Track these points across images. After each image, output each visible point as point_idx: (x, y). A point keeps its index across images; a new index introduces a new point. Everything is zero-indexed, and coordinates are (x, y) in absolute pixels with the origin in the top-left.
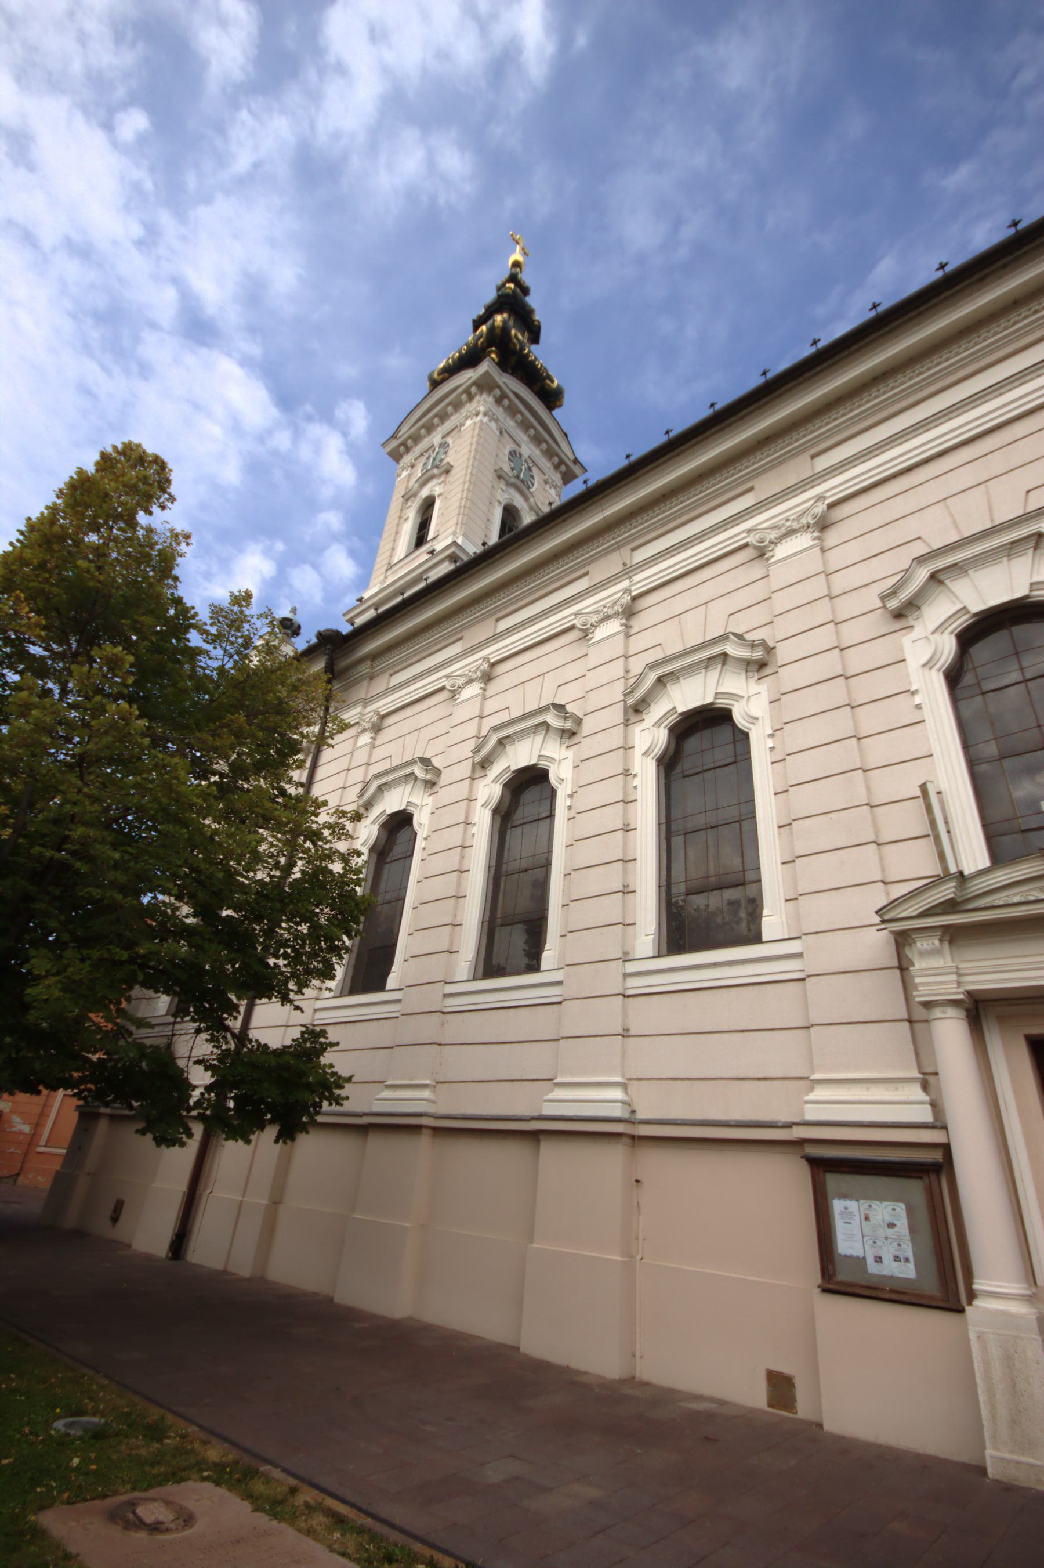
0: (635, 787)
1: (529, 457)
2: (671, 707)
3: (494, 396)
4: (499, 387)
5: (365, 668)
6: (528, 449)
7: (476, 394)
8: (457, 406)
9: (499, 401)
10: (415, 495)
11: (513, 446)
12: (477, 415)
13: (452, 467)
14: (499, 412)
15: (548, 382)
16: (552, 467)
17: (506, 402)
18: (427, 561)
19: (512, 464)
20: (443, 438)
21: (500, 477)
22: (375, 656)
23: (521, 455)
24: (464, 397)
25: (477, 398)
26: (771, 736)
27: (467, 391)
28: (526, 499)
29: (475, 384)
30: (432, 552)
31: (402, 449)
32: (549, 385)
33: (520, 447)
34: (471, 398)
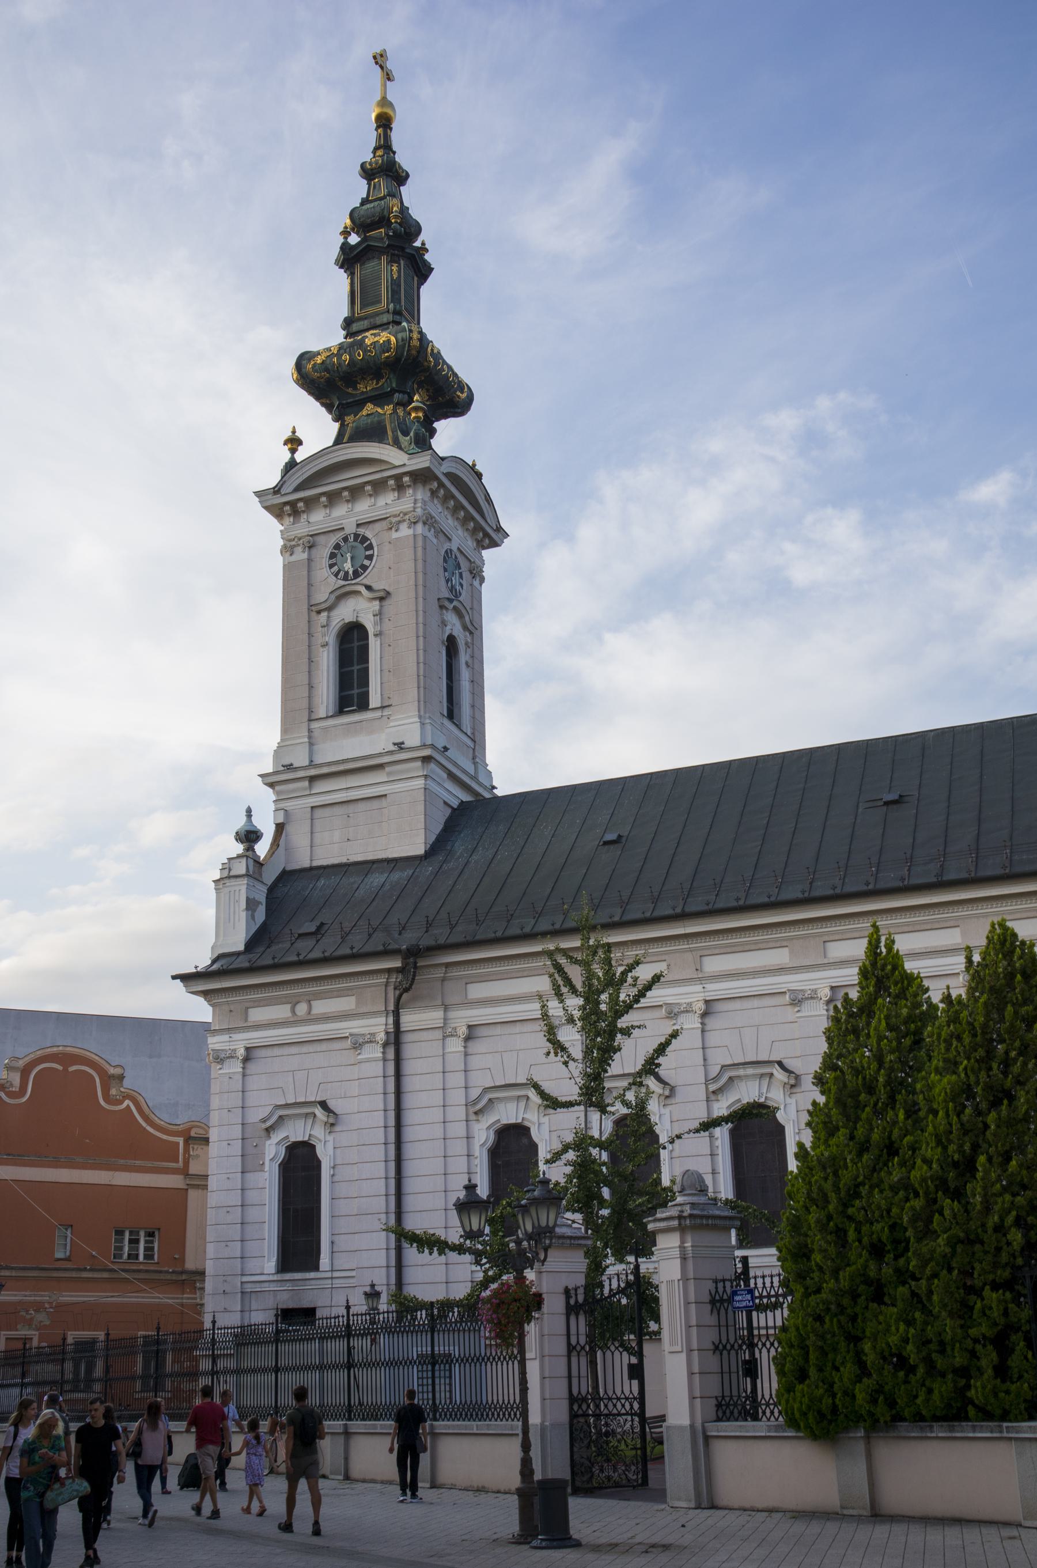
0: (717, 1147)
1: (458, 549)
2: (737, 1098)
3: (431, 490)
4: (436, 478)
5: (439, 973)
6: (460, 539)
7: (409, 486)
9: (434, 493)
10: (329, 609)
11: (447, 546)
12: (415, 523)
13: (388, 593)
14: (436, 509)
15: (458, 393)
16: (475, 544)
17: (442, 492)
18: (391, 753)
19: (446, 574)
20: (358, 525)
21: (442, 607)
22: (448, 965)
23: (451, 550)
24: (391, 482)
25: (411, 491)
26: (798, 1133)
27: (398, 478)
28: (460, 615)
29: (411, 474)
30: (400, 746)
31: (287, 508)
32: (459, 397)
33: (450, 540)
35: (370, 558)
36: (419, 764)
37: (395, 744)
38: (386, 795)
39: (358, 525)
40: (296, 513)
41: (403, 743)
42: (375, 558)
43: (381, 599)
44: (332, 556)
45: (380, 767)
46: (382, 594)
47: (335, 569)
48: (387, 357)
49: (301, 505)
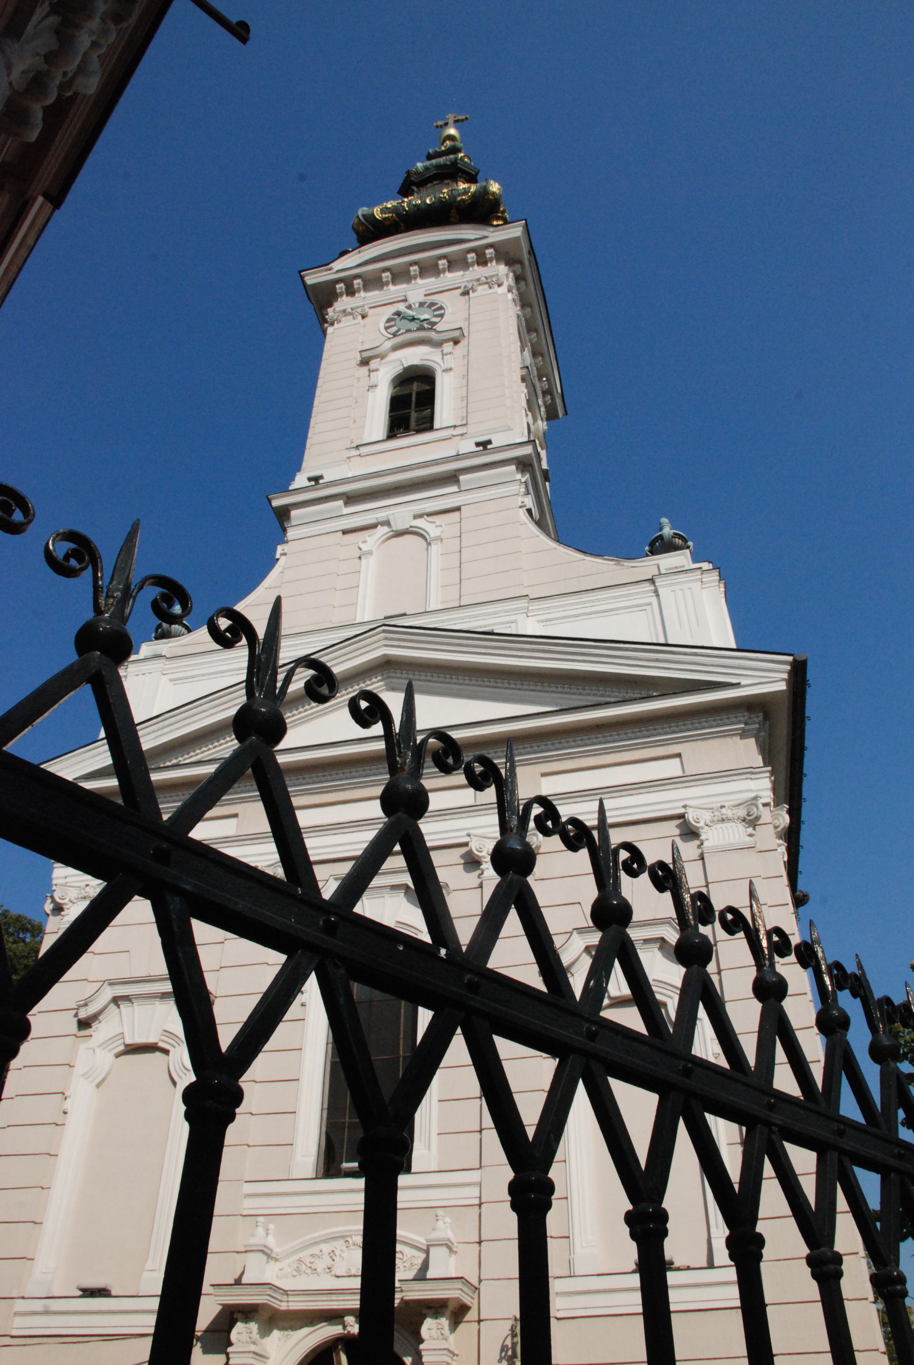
8: (457, 263)
24: (471, 257)
31: (340, 287)
34: (482, 261)
35: (442, 316)
36: (513, 468)
37: (478, 444)
38: (458, 509)
39: (426, 295)
40: (351, 292)
41: (489, 442)
42: (445, 317)
43: (456, 342)
44: (389, 320)
45: (452, 478)
46: (456, 334)
47: (394, 329)
48: (463, 200)
49: (357, 283)
